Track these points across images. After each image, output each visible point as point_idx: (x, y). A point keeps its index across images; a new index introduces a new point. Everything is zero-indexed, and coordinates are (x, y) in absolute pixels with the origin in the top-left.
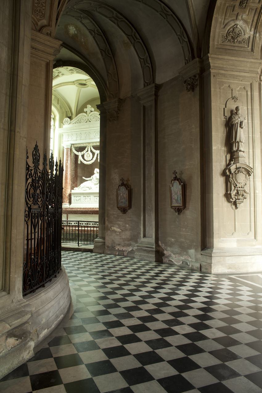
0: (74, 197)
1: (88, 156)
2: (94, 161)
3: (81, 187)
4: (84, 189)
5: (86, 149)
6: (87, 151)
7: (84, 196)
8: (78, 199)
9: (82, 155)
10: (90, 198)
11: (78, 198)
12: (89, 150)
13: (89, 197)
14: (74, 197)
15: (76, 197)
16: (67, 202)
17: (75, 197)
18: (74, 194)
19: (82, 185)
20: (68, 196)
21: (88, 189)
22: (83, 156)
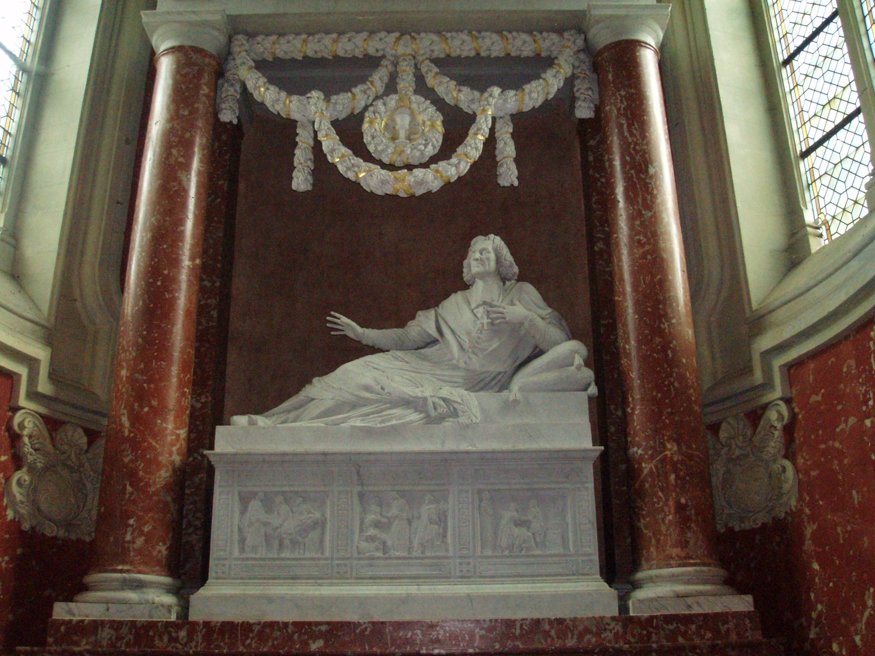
0: (245, 500)
1: (403, 122)
2: (464, 168)
3: (314, 409)
4: (374, 422)
5: (379, 79)
6: (391, 87)
7: (361, 495)
8: (290, 525)
9: (335, 123)
10: (442, 519)
11: (287, 520)
12: (406, 82)
13: (427, 510)
14: (245, 500)
15: (268, 504)
16: (148, 562)
17: (255, 506)
18: (243, 464)
19: (325, 389)
20: (167, 487)
21: (414, 416)
22: (350, 131)
